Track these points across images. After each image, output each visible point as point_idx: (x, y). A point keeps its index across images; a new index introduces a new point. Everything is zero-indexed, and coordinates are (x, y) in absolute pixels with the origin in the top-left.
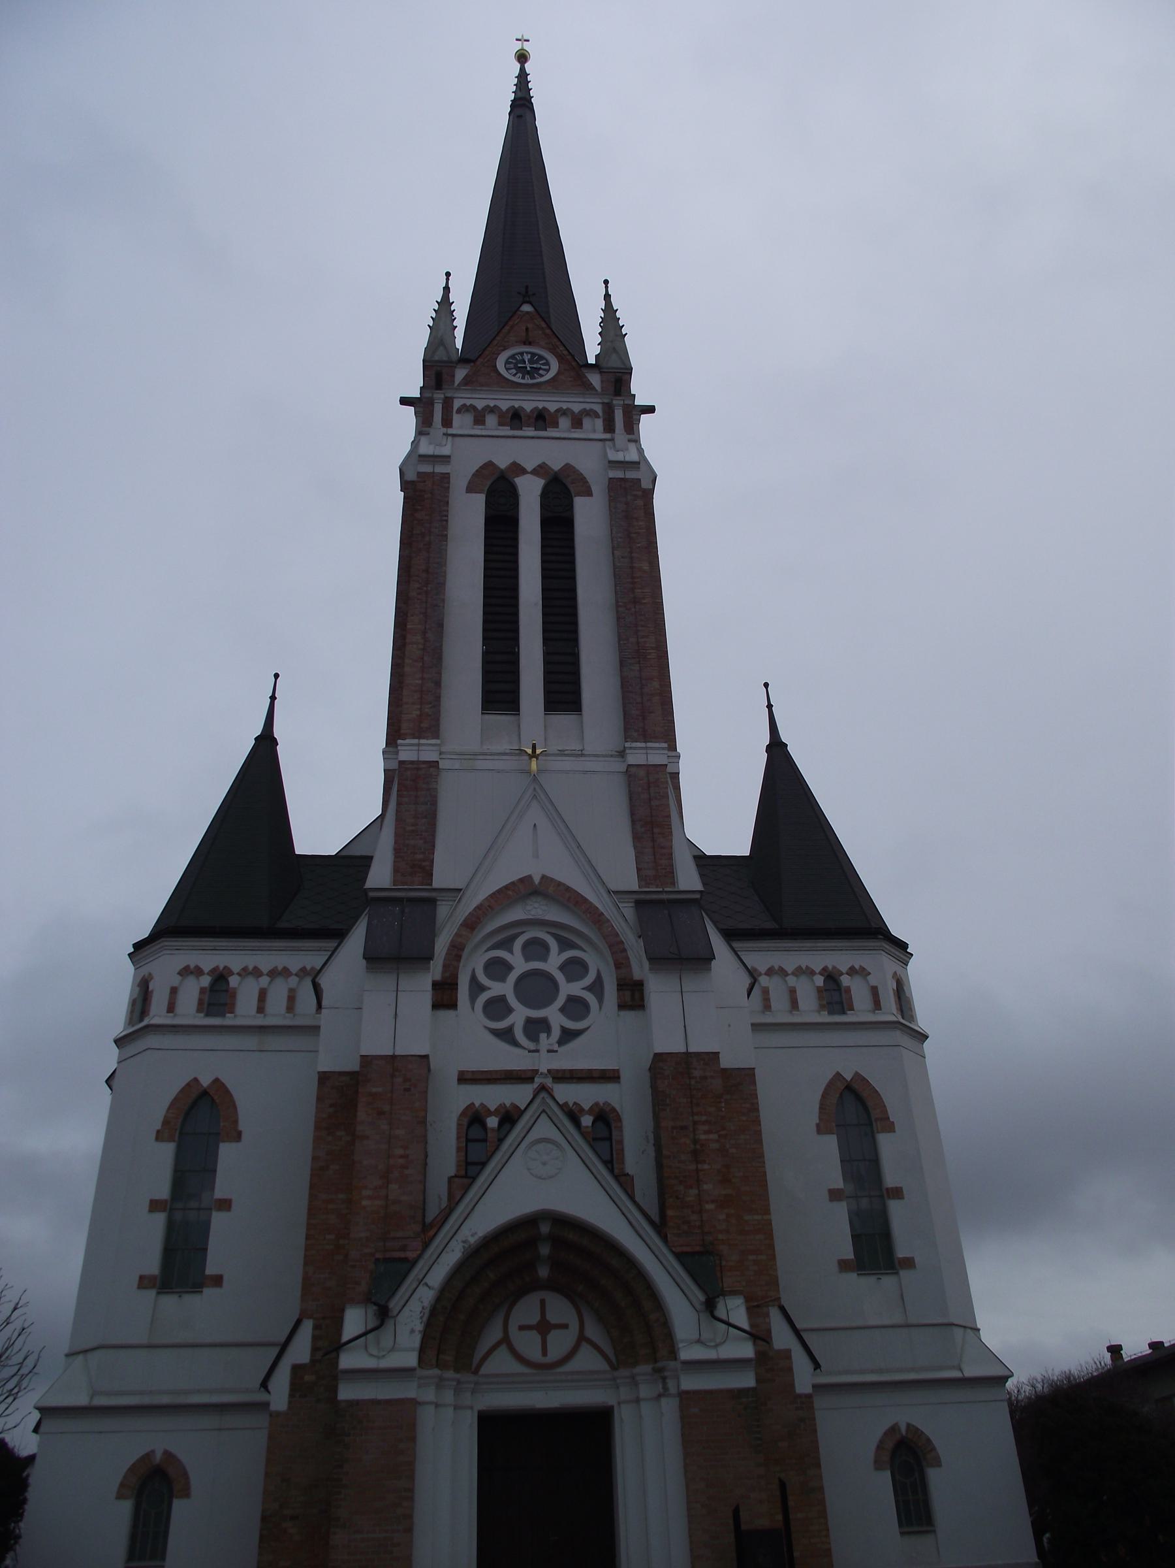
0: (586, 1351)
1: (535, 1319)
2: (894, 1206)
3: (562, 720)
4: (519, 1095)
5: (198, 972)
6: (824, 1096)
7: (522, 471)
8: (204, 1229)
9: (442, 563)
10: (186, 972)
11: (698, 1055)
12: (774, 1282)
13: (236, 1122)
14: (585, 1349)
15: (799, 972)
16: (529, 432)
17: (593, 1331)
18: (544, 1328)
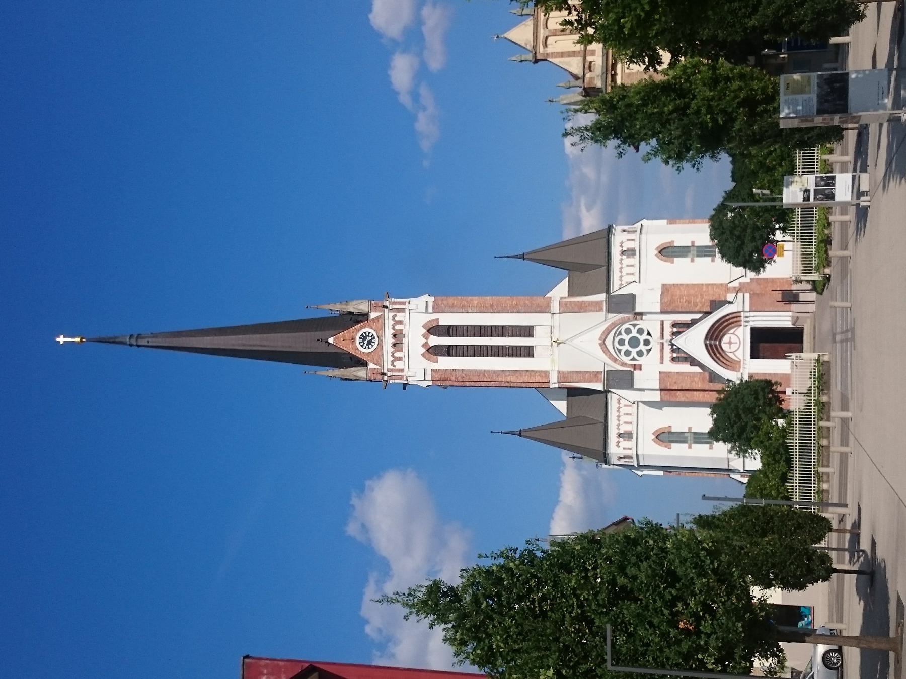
0: (736, 333)
1: (728, 345)
2: (696, 244)
3: (537, 331)
4: (667, 348)
5: (618, 442)
6: (662, 260)
7: (426, 343)
8: (695, 433)
9: (470, 371)
10: (618, 446)
11: (661, 300)
12: (722, 284)
13: (666, 428)
14: (736, 333)
15: (621, 263)
16: (405, 340)
17: (732, 331)
18: (730, 343)
